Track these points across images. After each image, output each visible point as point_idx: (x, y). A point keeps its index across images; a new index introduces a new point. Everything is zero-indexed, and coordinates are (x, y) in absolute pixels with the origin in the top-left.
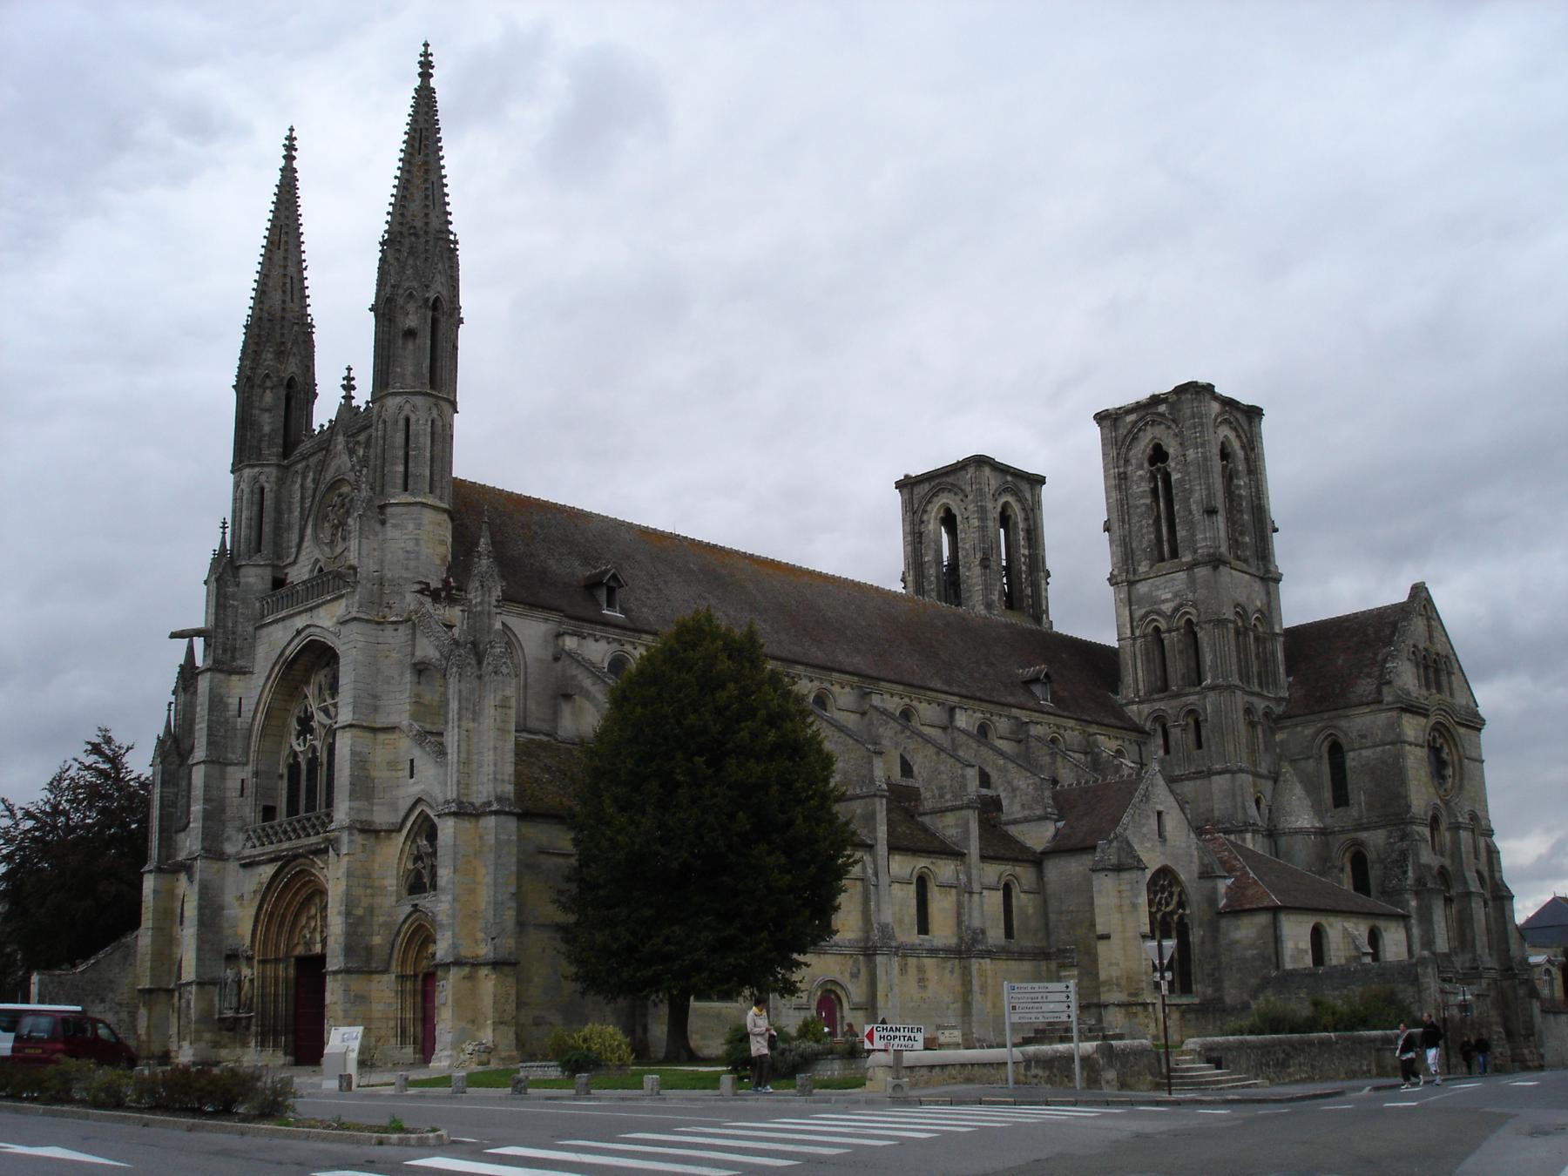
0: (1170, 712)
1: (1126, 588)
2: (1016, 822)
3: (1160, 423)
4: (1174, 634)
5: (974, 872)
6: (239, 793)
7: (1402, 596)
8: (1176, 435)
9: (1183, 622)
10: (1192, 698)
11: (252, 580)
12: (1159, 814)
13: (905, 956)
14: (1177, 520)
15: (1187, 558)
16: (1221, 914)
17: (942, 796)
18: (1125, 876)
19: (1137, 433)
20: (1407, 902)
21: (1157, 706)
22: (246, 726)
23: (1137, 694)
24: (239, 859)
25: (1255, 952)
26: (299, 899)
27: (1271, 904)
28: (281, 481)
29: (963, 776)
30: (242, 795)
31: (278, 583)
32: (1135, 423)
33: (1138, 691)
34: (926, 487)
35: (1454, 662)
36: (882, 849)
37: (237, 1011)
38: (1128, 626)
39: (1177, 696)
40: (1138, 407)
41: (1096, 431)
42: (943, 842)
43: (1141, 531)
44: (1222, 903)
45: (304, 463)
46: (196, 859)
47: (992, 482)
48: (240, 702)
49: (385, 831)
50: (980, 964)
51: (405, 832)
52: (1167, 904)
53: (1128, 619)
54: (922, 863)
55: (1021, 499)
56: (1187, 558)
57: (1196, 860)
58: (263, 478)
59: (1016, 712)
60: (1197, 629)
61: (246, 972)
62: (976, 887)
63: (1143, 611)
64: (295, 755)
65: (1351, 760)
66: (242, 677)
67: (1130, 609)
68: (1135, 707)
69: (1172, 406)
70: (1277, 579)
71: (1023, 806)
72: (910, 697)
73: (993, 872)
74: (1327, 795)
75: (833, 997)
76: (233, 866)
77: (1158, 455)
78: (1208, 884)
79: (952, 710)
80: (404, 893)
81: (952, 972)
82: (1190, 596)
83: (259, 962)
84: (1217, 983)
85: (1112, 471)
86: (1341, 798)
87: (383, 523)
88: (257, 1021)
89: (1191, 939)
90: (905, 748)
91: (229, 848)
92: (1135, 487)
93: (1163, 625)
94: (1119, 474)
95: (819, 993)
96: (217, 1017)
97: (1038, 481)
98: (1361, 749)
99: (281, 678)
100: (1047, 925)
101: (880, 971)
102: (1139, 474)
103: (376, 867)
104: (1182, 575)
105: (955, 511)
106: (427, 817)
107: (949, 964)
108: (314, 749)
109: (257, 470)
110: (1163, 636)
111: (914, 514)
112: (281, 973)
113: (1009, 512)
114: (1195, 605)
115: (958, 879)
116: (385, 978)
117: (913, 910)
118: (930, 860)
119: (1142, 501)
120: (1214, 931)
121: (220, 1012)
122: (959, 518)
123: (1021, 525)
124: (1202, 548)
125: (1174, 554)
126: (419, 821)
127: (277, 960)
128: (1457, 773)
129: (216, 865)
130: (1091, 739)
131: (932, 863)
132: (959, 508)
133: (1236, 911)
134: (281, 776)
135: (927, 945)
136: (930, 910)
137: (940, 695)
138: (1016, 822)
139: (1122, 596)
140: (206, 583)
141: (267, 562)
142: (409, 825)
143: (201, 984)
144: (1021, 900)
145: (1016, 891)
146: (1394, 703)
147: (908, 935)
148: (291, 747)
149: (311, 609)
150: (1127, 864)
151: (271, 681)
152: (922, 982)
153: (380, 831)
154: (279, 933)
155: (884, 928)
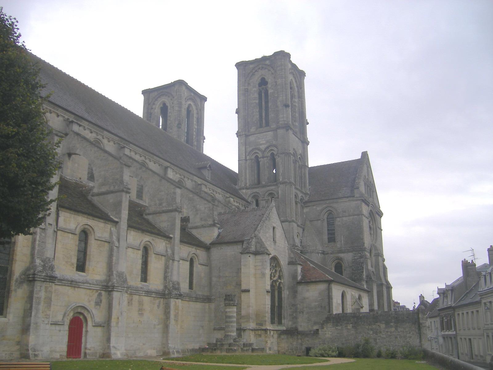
0: (261, 193)
1: (244, 138)
2: (196, 228)
3: (266, 68)
5: (176, 248)
7: (359, 157)
9: (269, 154)
10: (273, 187)
12: (274, 228)
13: (131, 294)
14: (270, 110)
15: (273, 126)
16: (300, 283)
17: (160, 204)
18: (259, 257)
19: (254, 72)
20: (363, 285)
21: (255, 190)
23: (245, 185)
25: (317, 304)
27: (326, 279)
29: (175, 193)
32: (254, 68)
33: (246, 183)
34: (156, 93)
35: (374, 187)
36: (124, 224)
38: (244, 154)
39: (264, 186)
40: (256, 60)
41: (235, 71)
42: (159, 230)
44: (299, 278)
47: (186, 93)
50: (176, 302)
52: (274, 276)
53: (244, 151)
54: (147, 238)
55: (196, 105)
56: (273, 126)
57: (287, 255)
59: (195, 178)
60: (276, 157)
62: (177, 258)
63: (251, 149)
65: (338, 222)
67: (245, 147)
68: (244, 191)
70: (308, 143)
71: (201, 219)
72: (145, 157)
73: (186, 251)
74: (326, 237)
75: (81, 317)
77: (263, 82)
78: (292, 267)
79: (166, 168)
81: (158, 306)
82: (274, 142)
84: (294, 319)
86: (332, 239)
89: (283, 296)
90: (141, 177)
93: (260, 155)
94: (245, 89)
95: (72, 314)
97: (204, 99)
98: (343, 217)
100: (210, 283)
101: (115, 303)
102: (254, 91)
104: (271, 133)
105: (168, 104)
107: (157, 301)
110: (260, 160)
111: (149, 104)
113: (191, 109)
115: (167, 251)
117: (139, 266)
118: (152, 238)
119: (254, 101)
120: (294, 293)
122: (169, 107)
123: (195, 115)
125: (267, 124)
128: (375, 233)
130: (227, 199)
131: (153, 240)
133: (306, 281)
135: (145, 289)
136: (149, 267)
137: (161, 160)
138: (196, 228)
139: (242, 141)
144: (198, 268)
145: (196, 264)
146: (360, 197)
147: (135, 281)
150: (260, 252)
152: (141, 312)
155: (121, 275)
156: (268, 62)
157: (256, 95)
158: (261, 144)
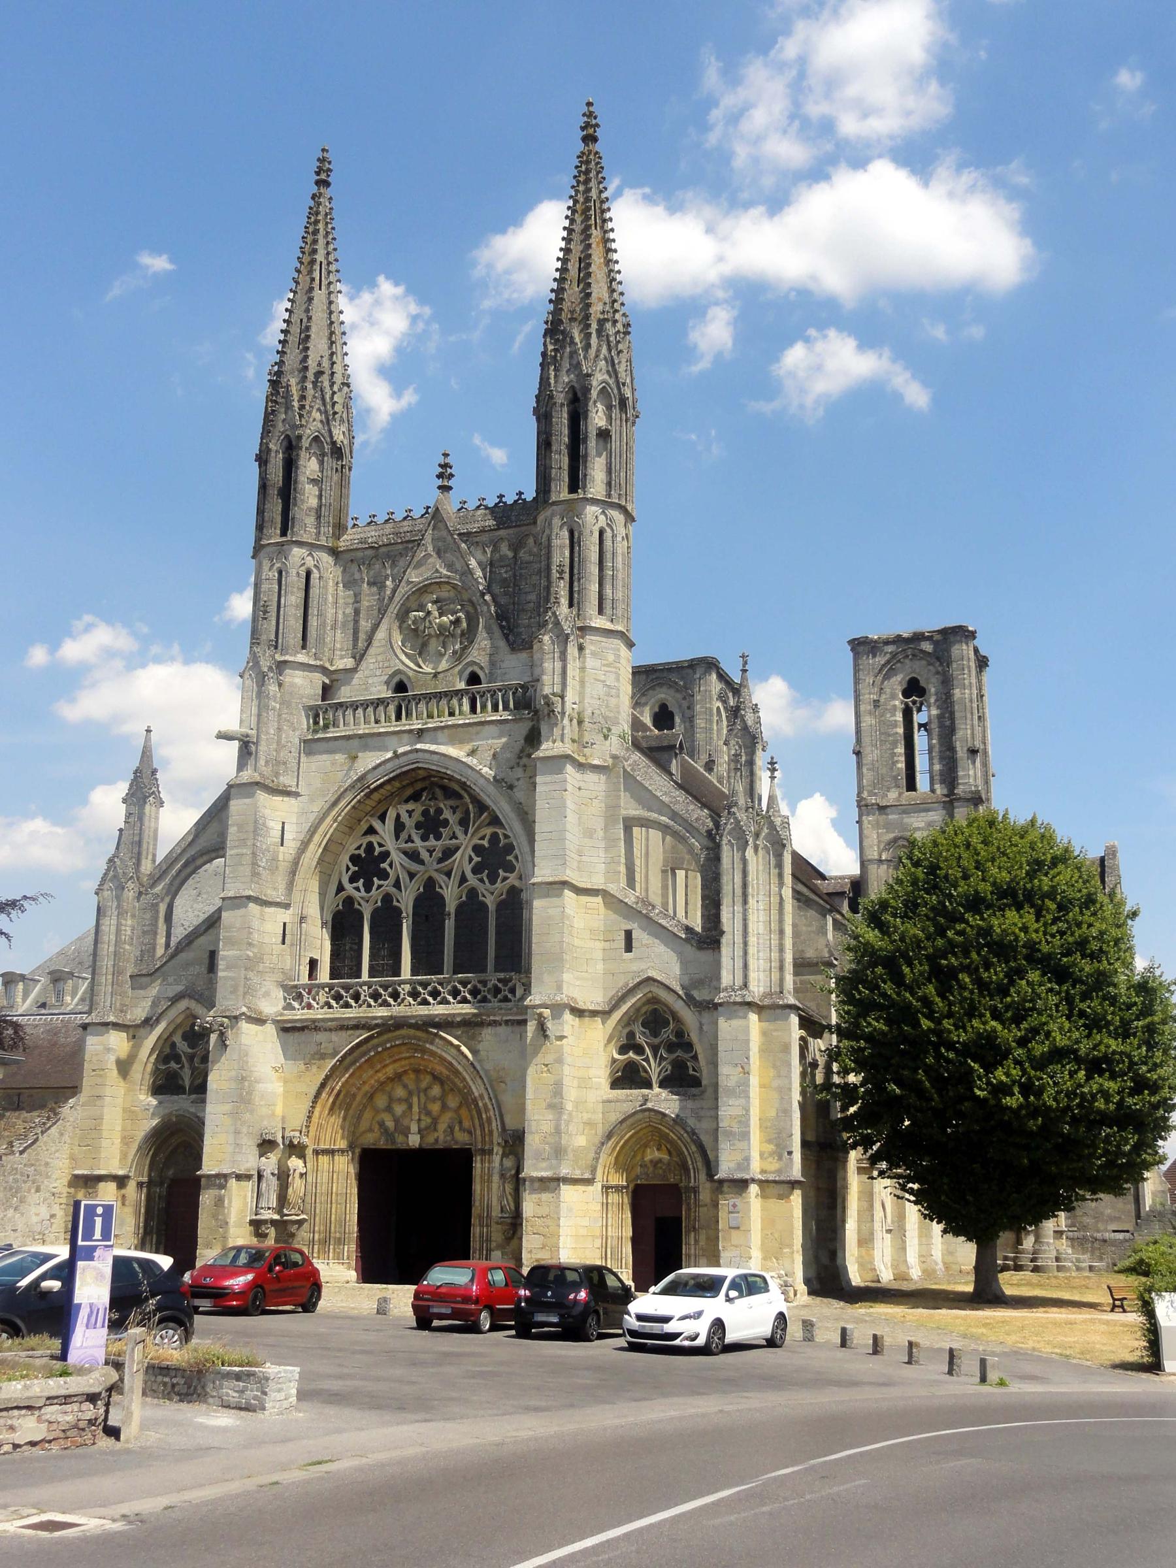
3: (921, 659)
8: (938, 673)
22: (290, 858)
43: (893, 757)
48: (283, 828)
51: (617, 1015)
69: (936, 644)
85: (867, 696)
92: (888, 716)
99: (353, 807)
105: (672, 707)
108: (387, 898)
124: (963, 784)
132: (680, 706)
148: (341, 888)
156: (927, 647)
157: (899, 717)
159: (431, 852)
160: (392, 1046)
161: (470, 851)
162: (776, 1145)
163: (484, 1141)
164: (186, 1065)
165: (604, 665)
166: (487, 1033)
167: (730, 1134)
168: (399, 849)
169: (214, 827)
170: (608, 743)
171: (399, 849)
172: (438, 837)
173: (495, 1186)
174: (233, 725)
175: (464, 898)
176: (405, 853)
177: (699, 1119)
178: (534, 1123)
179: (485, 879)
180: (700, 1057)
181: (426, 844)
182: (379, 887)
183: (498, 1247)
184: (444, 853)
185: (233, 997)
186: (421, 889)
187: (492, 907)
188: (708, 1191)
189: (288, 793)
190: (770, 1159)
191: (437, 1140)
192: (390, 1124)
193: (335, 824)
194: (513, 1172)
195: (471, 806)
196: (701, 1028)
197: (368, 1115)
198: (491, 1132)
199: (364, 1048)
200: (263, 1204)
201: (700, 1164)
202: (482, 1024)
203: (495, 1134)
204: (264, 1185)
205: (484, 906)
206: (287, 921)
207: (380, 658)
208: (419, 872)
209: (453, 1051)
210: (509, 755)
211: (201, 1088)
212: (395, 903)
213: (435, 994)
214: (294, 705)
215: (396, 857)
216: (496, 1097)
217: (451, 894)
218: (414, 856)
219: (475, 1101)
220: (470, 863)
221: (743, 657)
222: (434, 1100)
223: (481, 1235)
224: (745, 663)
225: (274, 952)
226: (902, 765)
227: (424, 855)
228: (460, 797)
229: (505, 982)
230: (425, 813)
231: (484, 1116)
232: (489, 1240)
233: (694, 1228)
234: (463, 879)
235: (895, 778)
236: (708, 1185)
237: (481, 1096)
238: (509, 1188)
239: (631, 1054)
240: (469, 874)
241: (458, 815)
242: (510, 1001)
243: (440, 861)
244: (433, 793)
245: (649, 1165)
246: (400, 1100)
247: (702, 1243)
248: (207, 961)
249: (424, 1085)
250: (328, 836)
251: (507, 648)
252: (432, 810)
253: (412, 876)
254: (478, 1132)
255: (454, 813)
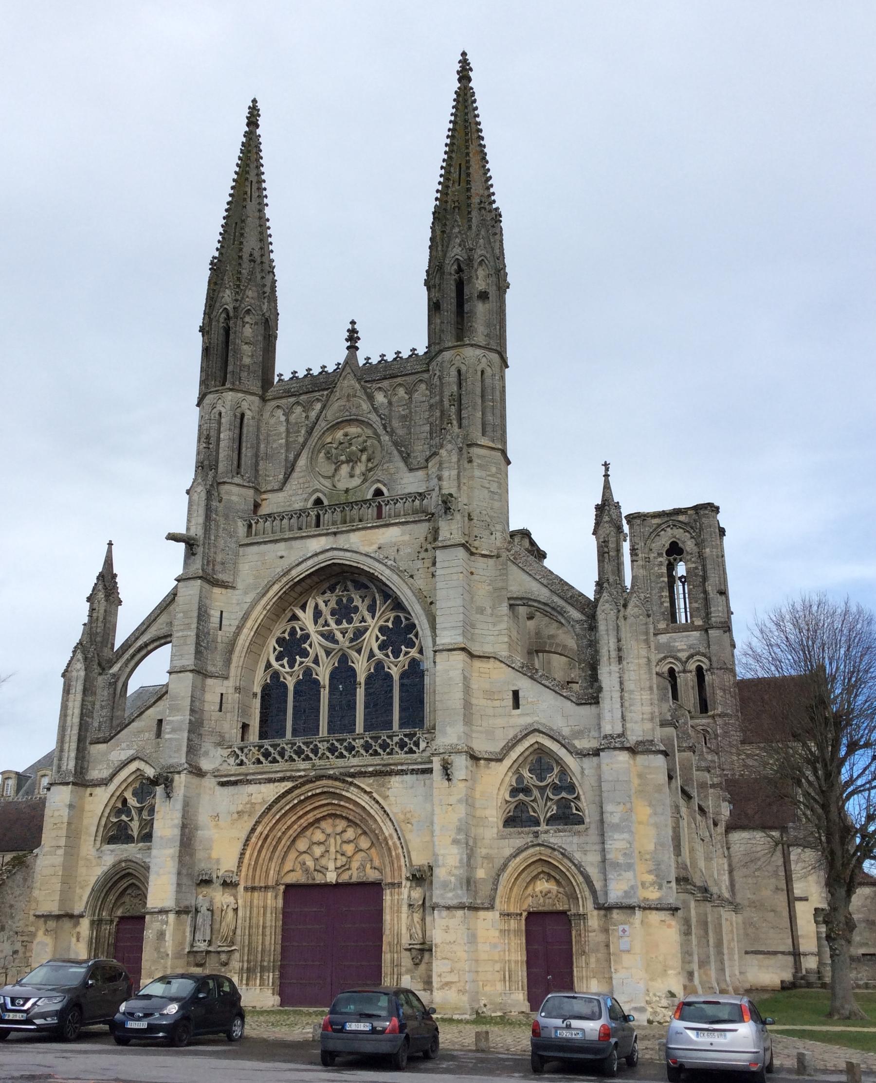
4: (689, 674)
6: (218, 707)
8: (692, 538)
10: (704, 721)
11: (234, 498)
22: (226, 640)
24: (215, 776)
26: (303, 822)
28: (261, 412)
30: (220, 710)
31: (257, 506)
32: (659, 525)
37: (210, 943)
45: (292, 400)
46: (179, 773)
49: (486, 759)
58: (245, 405)
61: (221, 898)
63: (662, 655)
64: (276, 675)
66: (224, 591)
76: (209, 782)
80: (501, 825)
82: (702, 650)
83: (246, 889)
87: (470, 461)
88: (242, 956)
91: (206, 765)
96: (187, 950)
99: (280, 597)
103: (478, 796)
106: (540, 751)
108: (308, 672)
109: (240, 395)
112: (270, 902)
114: (704, 655)
116: (489, 915)
121: (192, 946)
126: (527, 753)
127: (266, 888)
129: (195, 780)
134: (255, 695)
140: (188, 492)
141: (251, 485)
142: (514, 755)
143: (178, 913)
148: (269, 665)
149: (335, 534)
151: (265, 599)
153: (479, 759)
154: (271, 859)
156: (682, 518)
157: (664, 570)
158: (679, 651)
159: (344, 634)
160: (313, 795)
161: (376, 631)
162: (656, 876)
163: (393, 876)
164: (136, 818)
165: (489, 476)
166: (395, 781)
167: (616, 865)
168: (317, 632)
169: (163, 619)
170: (493, 537)
171: (317, 632)
172: (350, 621)
173: (404, 916)
174: (182, 530)
175: (372, 670)
176: (323, 635)
177: (585, 852)
178: (440, 858)
179: (390, 654)
180: (582, 797)
181: (340, 627)
182: (302, 663)
183: (408, 971)
184: (354, 634)
185: (176, 755)
186: (336, 665)
187: (396, 677)
188: (596, 918)
189: (226, 587)
190: (651, 889)
191: (351, 878)
192: (310, 863)
193: (265, 612)
194: (421, 903)
195: (377, 596)
196: (582, 773)
197: (292, 855)
198: (400, 868)
199: (289, 797)
200: (198, 936)
201: (587, 893)
202: (390, 773)
203: (404, 869)
204: (200, 920)
205: (389, 676)
206: (224, 692)
207: (301, 481)
208: (334, 649)
209: (366, 797)
210: (409, 550)
211: (147, 837)
212: (314, 676)
213: (350, 749)
214: (231, 517)
215: (315, 638)
216: (404, 837)
217: (361, 667)
218: (329, 637)
219: (386, 839)
220: (377, 641)
221: (606, 465)
222: (349, 842)
223: (392, 961)
224: (607, 469)
225: (213, 718)
226: (667, 604)
227: (339, 636)
228: (367, 587)
229: (410, 736)
230: (339, 602)
231: (394, 854)
232: (399, 965)
233: (584, 952)
234: (372, 655)
235: (663, 613)
236: (595, 912)
237: (391, 835)
238: (417, 917)
239: (521, 796)
240: (376, 651)
241: (367, 601)
242: (415, 752)
243: (352, 640)
244: (345, 587)
245: (540, 895)
246: (319, 843)
247: (593, 965)
248: (155, 729)
249: (339, 829)
250: (259, 621)
251: (406, 469)
252: (345, 600)
253: (328, 653)
254: (388, 869)
255: (363, 601)
